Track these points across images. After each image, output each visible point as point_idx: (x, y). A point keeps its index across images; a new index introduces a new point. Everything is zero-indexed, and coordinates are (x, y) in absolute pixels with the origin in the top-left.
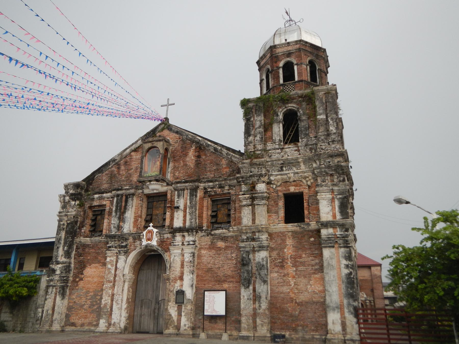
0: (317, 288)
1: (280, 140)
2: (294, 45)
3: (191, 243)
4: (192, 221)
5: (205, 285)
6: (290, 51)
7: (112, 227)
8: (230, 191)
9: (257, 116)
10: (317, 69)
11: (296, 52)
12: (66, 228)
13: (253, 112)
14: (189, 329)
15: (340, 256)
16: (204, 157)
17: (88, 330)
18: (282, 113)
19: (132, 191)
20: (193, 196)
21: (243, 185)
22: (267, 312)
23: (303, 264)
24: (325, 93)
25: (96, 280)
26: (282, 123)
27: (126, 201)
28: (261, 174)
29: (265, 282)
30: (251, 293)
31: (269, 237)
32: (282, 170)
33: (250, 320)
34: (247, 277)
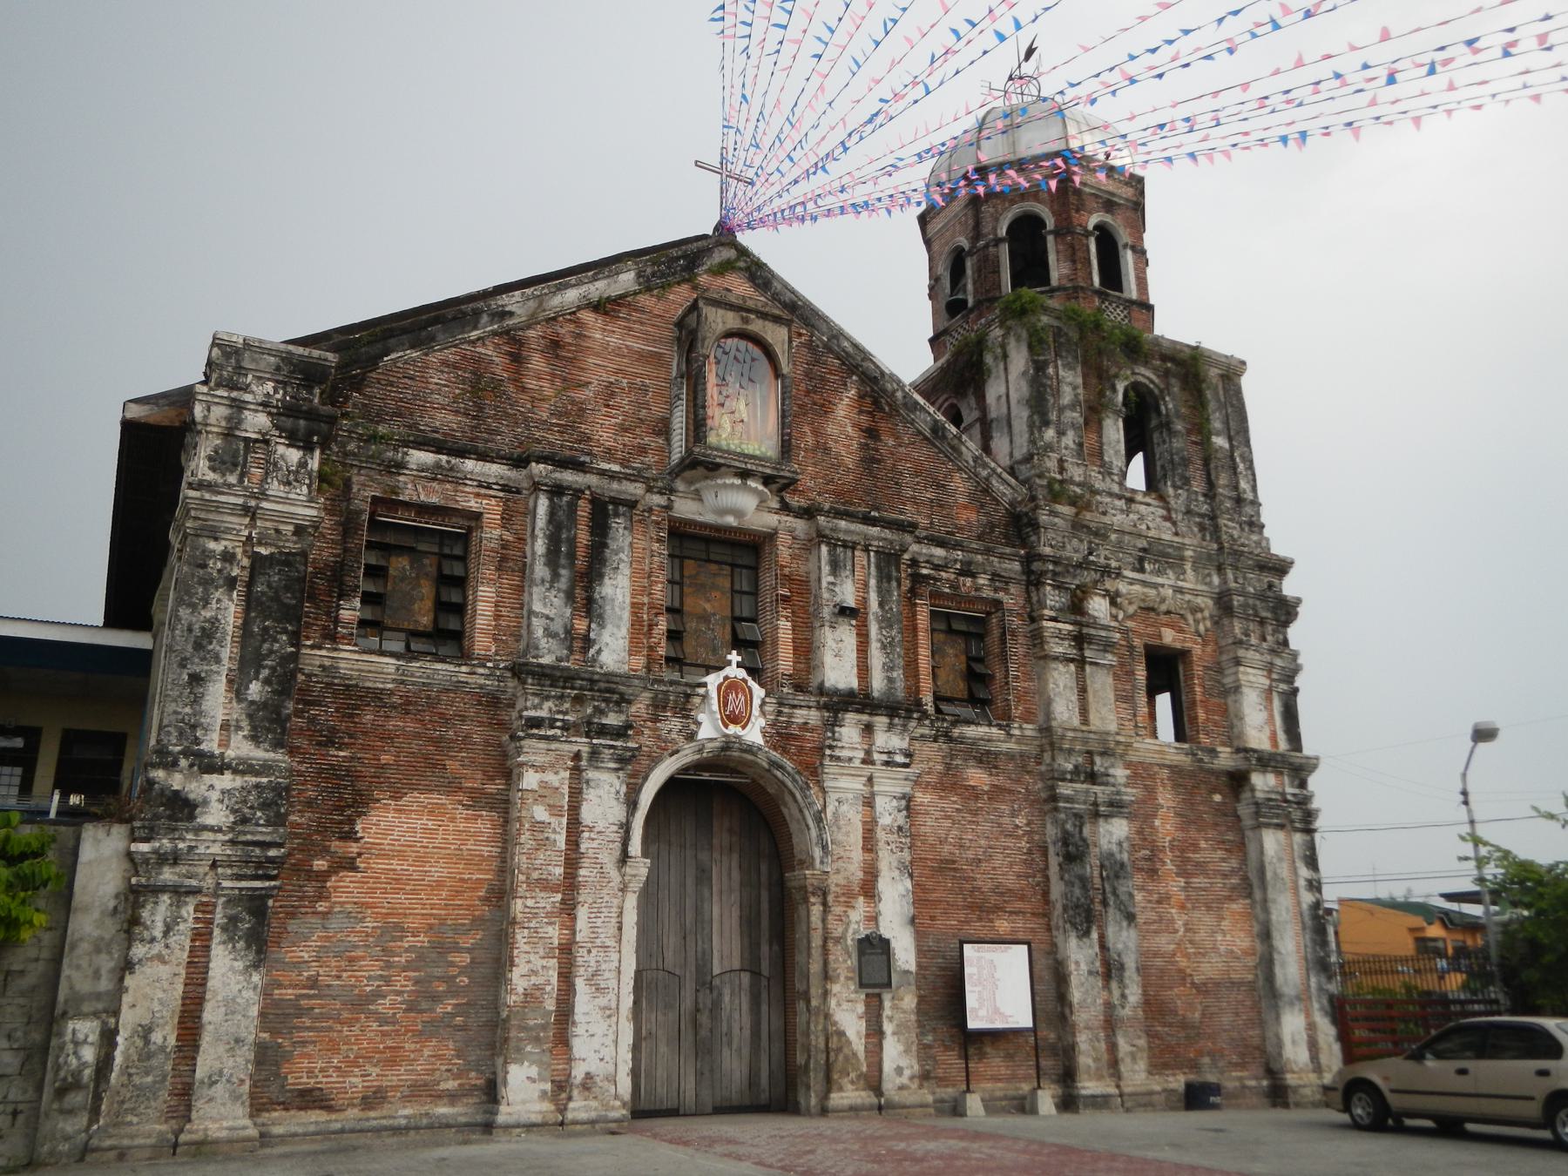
3: (900, 759)
4: (895, 674)
5: (933, 918)
7: (539, 633)
8: (1001, 595)
9: (1064, 366)
12: (250, 584)
14: (914, 1086)
16: (891, 442)
17: (425, 1121)
19: (635, 489)
20: (889, 581)
21: (1048, 588)
23: (1201, 868)
25: (437, 871)
27: (600, 528)
29: (1130, 918)
32: (1142, 570)
33: (1098, 1041)
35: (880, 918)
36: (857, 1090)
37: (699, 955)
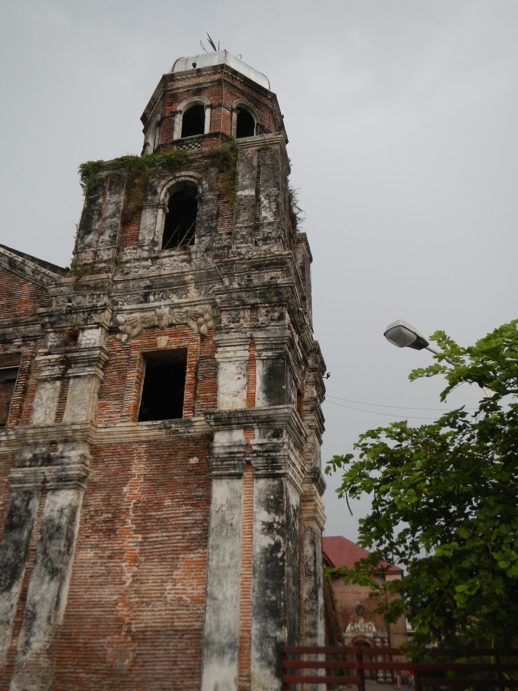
0: (189, 590)
1: (153, 241)
2: (209, 75)
6: (200, 84)
9: (110, 195)
10: (256, 123)
11: (213, 86)
13: (104, 188)
15: (255, 499)
18: (165, 188)
21: (51, 334)
22: (44, 662)
24: (259, 151)
26: (164, 210)
28: (94, 306)
30: (12, 606)
31: (90, 457)
32: (146, 300)
34: (13, 560)
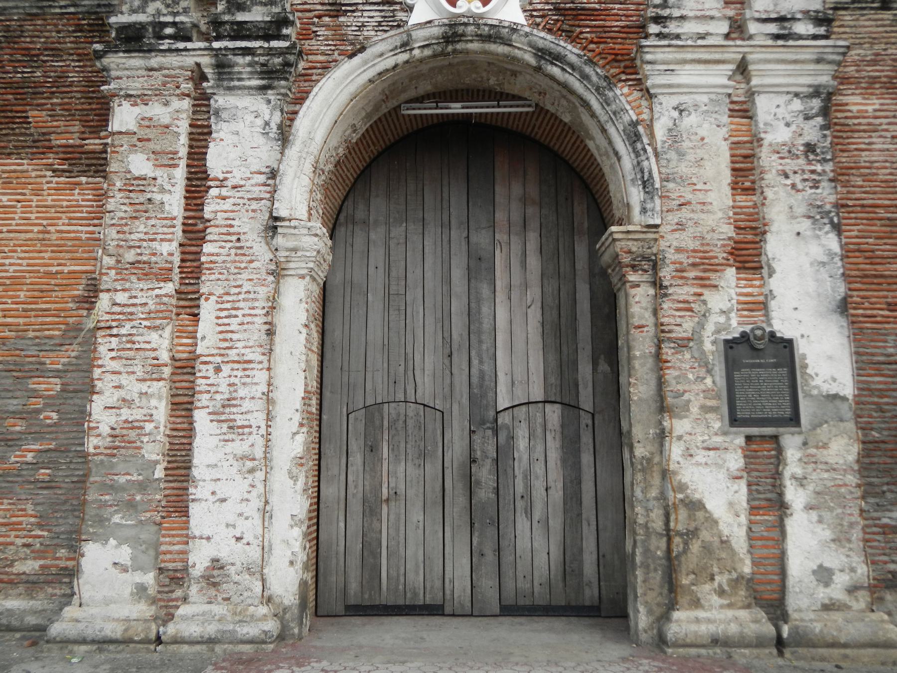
14: (861, 602)
35: (773, 304)
36: (730, 606)
37: (475, 380)
